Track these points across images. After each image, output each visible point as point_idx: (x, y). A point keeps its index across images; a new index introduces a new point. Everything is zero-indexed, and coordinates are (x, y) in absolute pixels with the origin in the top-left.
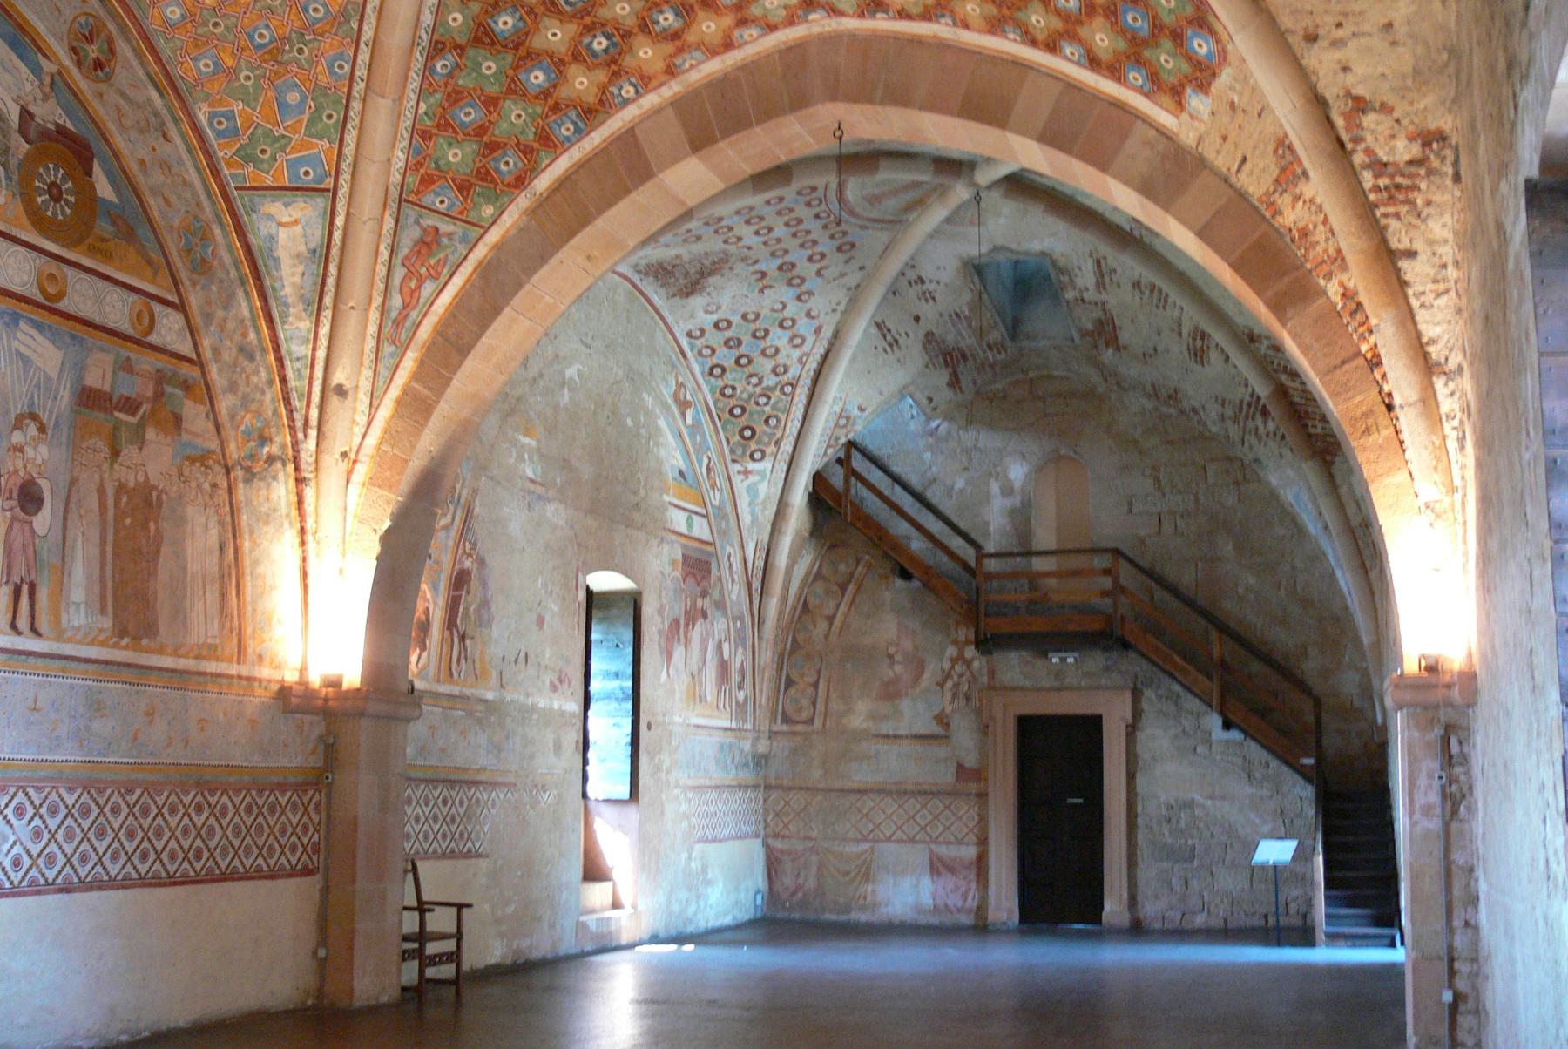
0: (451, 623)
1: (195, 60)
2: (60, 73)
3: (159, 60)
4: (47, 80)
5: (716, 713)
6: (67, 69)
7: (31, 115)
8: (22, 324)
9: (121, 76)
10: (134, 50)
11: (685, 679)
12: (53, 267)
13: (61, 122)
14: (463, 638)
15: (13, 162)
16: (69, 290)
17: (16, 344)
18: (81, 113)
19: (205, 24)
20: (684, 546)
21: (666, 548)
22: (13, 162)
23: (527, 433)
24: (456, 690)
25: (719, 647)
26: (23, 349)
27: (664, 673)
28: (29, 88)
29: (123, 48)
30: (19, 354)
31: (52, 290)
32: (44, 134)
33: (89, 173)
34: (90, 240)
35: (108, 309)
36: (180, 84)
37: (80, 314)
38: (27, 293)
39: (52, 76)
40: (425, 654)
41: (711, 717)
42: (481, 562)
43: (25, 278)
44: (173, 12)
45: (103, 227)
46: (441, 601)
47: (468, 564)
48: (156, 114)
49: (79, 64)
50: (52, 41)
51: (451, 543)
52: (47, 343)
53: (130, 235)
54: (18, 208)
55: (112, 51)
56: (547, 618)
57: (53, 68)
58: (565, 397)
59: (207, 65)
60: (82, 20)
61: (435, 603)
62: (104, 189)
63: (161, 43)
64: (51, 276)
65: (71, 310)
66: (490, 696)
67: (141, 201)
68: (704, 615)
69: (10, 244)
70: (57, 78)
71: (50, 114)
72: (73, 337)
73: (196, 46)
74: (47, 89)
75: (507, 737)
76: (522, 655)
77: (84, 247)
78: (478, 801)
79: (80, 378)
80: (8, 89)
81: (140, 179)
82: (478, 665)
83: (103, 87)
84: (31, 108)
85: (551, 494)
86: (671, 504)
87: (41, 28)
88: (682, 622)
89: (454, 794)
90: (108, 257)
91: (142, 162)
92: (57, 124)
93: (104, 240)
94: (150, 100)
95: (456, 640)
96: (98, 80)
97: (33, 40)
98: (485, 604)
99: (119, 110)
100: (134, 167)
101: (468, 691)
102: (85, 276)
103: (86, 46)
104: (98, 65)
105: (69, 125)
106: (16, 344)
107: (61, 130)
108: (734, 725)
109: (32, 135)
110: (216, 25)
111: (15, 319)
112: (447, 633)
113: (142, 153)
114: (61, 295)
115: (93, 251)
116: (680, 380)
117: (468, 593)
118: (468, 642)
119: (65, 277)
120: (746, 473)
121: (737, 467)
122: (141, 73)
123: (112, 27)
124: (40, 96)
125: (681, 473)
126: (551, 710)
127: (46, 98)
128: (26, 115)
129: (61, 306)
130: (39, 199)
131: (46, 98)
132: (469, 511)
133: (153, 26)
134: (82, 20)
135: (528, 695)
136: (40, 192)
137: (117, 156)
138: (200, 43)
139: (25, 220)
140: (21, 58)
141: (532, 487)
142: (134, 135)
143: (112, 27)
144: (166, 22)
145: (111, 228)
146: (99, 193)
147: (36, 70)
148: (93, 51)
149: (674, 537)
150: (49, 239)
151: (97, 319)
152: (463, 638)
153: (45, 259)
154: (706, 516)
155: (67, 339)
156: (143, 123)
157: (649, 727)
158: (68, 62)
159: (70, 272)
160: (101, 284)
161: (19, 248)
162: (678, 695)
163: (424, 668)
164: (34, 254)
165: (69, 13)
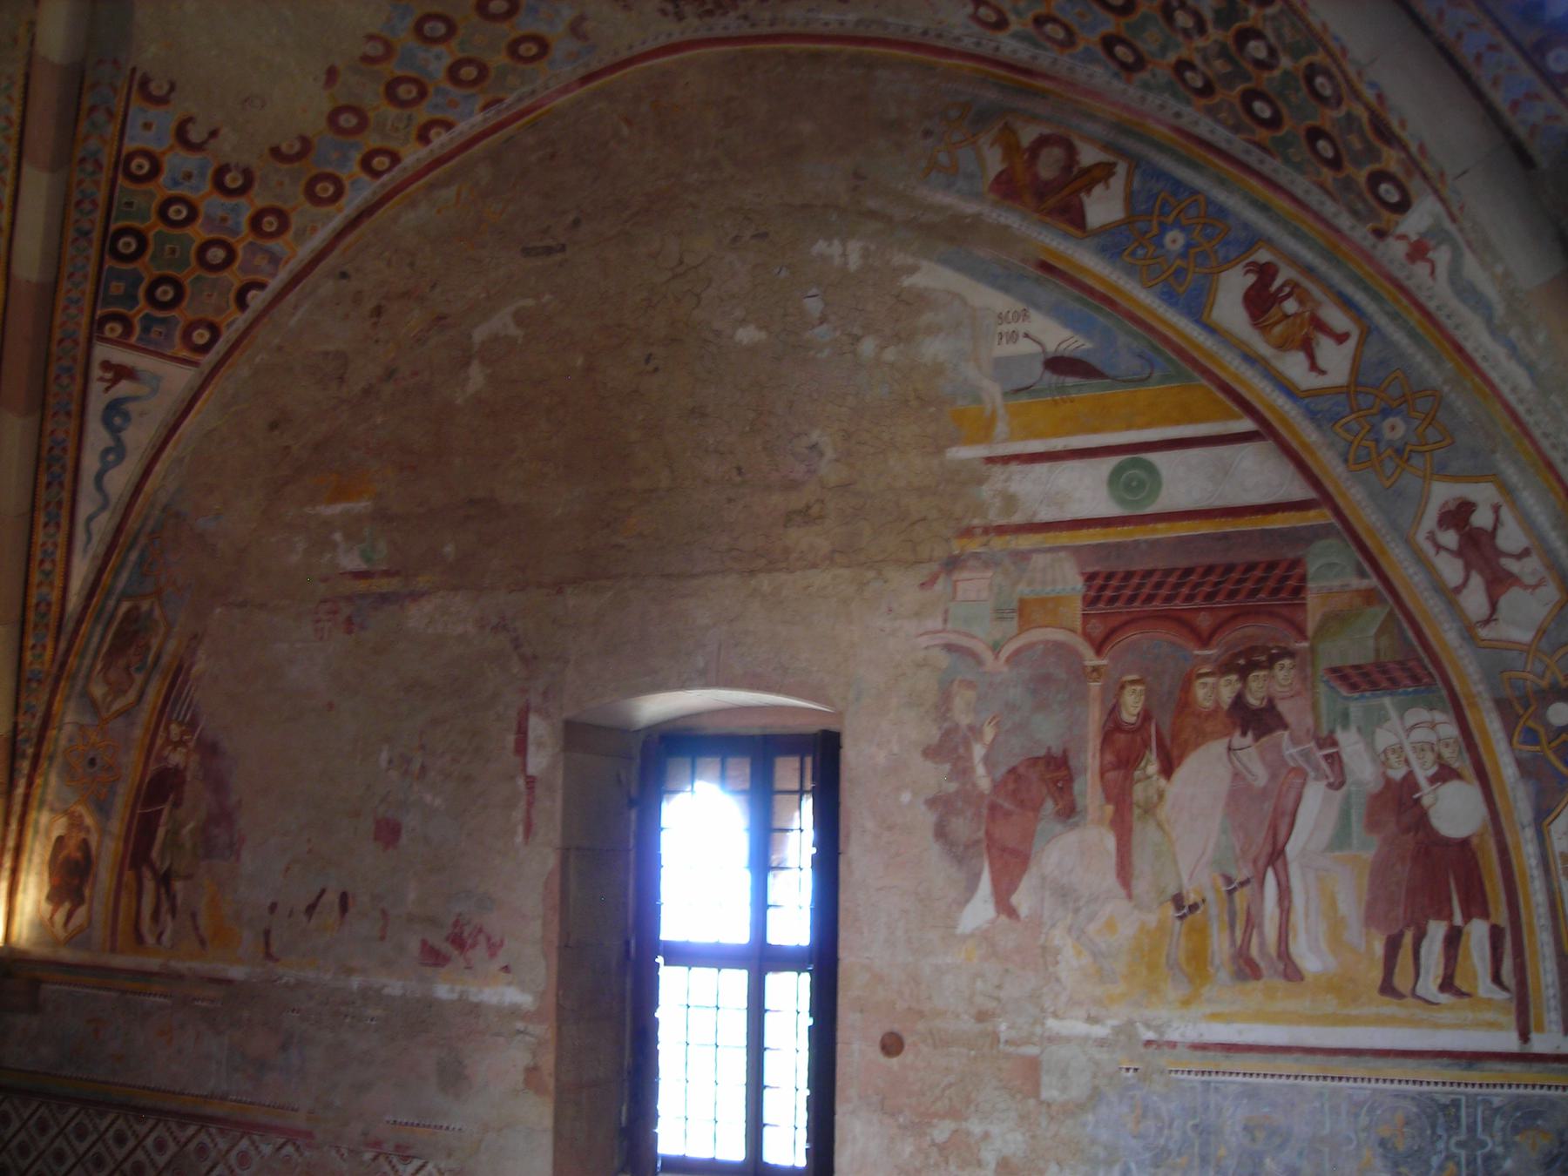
0: (138, 852)
5: (1390, 1007)
11: (1125, 922)
14: (165, 880)
20: (1076, 551)
21: (975, 586)
23: (340, 494)
24: (153, 963)
25: (1399, 804)
27: (980, 911)
40: (82, 911)
41: (1348, 1021)
42: (210, 750)
46: (116, 826)
47: (176, 758)
51: (138, 732)
56: (410, 821)
58: (477, 376)
61: (103, 831)
66: (237, 972)
68: (1257, 720)
75: (284, 1047)
76: (332, 898)
78: (202, 1150)
82: (203, 921)
85: (422, 582)
86: (990, 460)
88: (1090, 760)
89: (142, 1129)
95: (149, 885)
98: (223, 816)
101: (176, 965)
108: (1541, 1043)
112: (129, 875)
116: (1028, 135)
117: (177, 804)
118: (178, 885)
120: (1418, 251)
121: (1394, 251)
125: (1058, 364)
126: (430, 1003)
132: (179, 674)
135: (350, 971)
141: (361, 586)
149: (1025, 542)
152: (165, 880)
154: (1265, 431)
157: (892, 1045)
162: (1071, 962)
163: (80, 930)
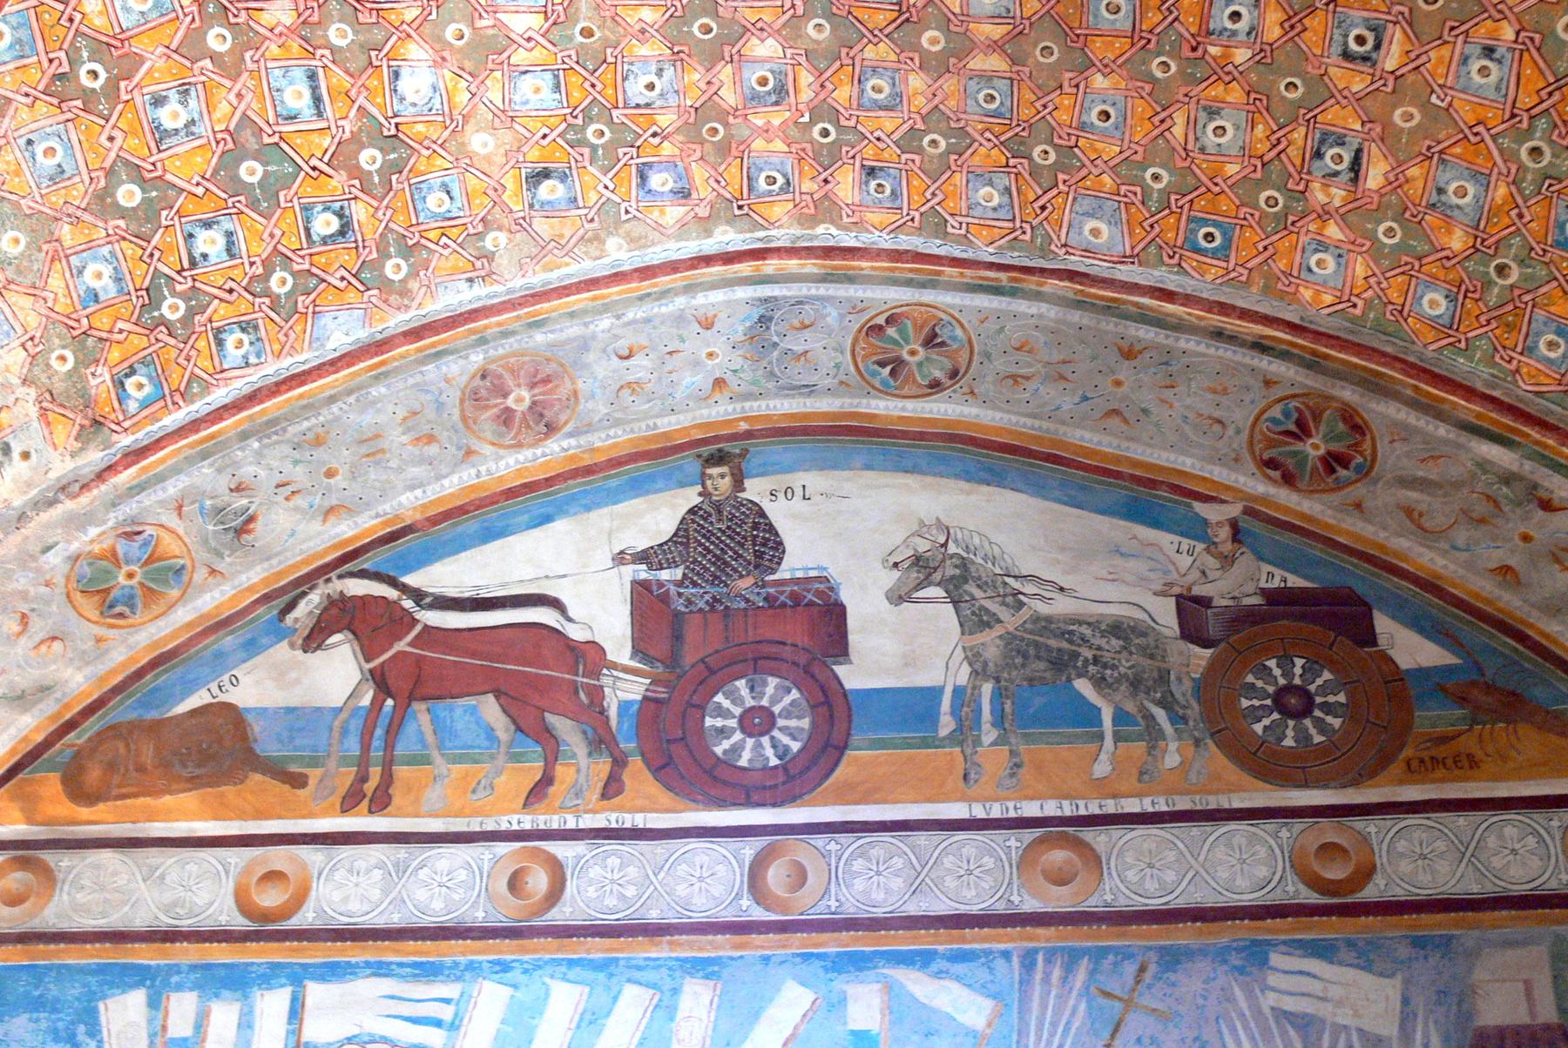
1: (1528, 350)
2: (1249, 512)
3: (1469, 392)
4: (1225, 533)
6: (1264, 500)
7: (1205, 602)
8: (1276, 959)
9: (1392, 457)
10: (1413, 404)
12: (1329, 832)
13: (1276, 583)
15: (1182, 690)
16: (1381, 859)
17: (1269, 1000)
18: (1317, 551)
19: (1488, 284)
22: (1182, 690)
26: (1290, 1004)
28: (1185, 561)
29: (1381, 412)
30: (1282, 1015)
31: (1335, 872)
32: (1242, 618)
33: (1369, 638)
34: (1408, 752)
35: (1497, 862)
36: (1537, 406)
37: (1423, 894)
38: (1277, 898)
39: (1234, 525)
43: (1262, 872)
44: (1433, 303)
45: (1433, 717)
48: (1508, 478)
49: (1288, 480)
50: (1219, 473)
52: (1350, 974)
53: (1511, 705)
54: (1215, 758)
55: (1356, 425)
57: (1234, 510)
59: (1551, 345)
60: (1276, 412)
62: (1409, 648)
63: (1460, 366)
64: (1329, 850)
65: (1399, 893)
67: (1521, 637)
69: (1207, 827)
70: (1246, 523)
71: (1240, 582)
72: (1418, 943)
73: (1510, 327)
74: (1227, 547)
77: (1396, 768)
79: (1466, 1015)
80: (1143, 580)
81: (1510, 602)
83: (1359, 491)
84: (1197, 591)
87: (1187, 463)
90: (1468, 765)
91: (1505, 570)
92: (1264, 592)
93: (1444, 739)
94: (1483, 465)
96: (1340, 486)
97: (1176, 489)
99: (1409, 511)
100: (1484, 588)
102: (1413, 820)
103: (1299, 446)
104: (1333, 462)
105: (1295, 581)
106: (1269, 1000)
107: (1278, 599)
109: (1213, 630)
110: (1502, 270)
111: (1257, 955)
113: (1497, 557)
114: (1366, 873)
115: (1418, 770)
119: (1365, 839)
122: (1443, 431)
123: (1348, 394)
124: (1211, 562)
127: (1227, 561)
128: (1191, 607)
129: (1371, 892)
130: (1258, 728)
131: (1227, 561)
133: (1429, 349)
134: (1276, 412)
136: (1256, 714)
137: (1431, 586)
138: (1512, 315)
139: (1232, 772)
140: (1156, 524)
142: (1461, 536)
143: (1348, 394)
144: (1433, 324)
145: (1459, 712)
146: (1404, 662)
147: (1197, 530)
148: (1314, 448)
150: (1305, 784)
151: (1473, 887)
153: (1299, 825)
155: (1404, 951)
156: (1481, 508)
158: (1260, 487)
159: (1371, 826)
160: (1462, 821)
161: (1233, 826)
164: (1271, 825)
165: (1241, 417)
